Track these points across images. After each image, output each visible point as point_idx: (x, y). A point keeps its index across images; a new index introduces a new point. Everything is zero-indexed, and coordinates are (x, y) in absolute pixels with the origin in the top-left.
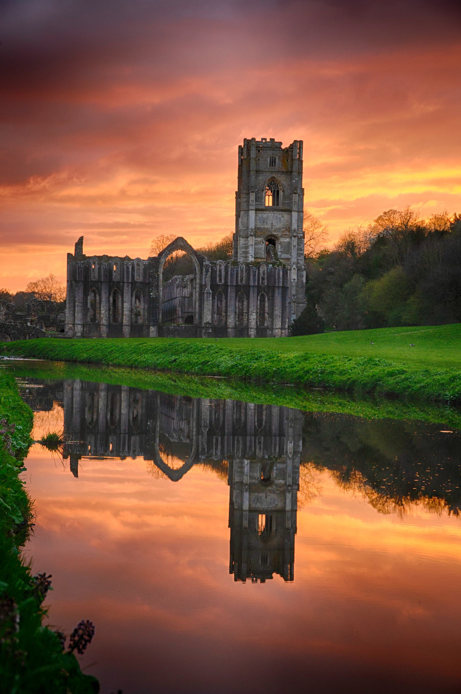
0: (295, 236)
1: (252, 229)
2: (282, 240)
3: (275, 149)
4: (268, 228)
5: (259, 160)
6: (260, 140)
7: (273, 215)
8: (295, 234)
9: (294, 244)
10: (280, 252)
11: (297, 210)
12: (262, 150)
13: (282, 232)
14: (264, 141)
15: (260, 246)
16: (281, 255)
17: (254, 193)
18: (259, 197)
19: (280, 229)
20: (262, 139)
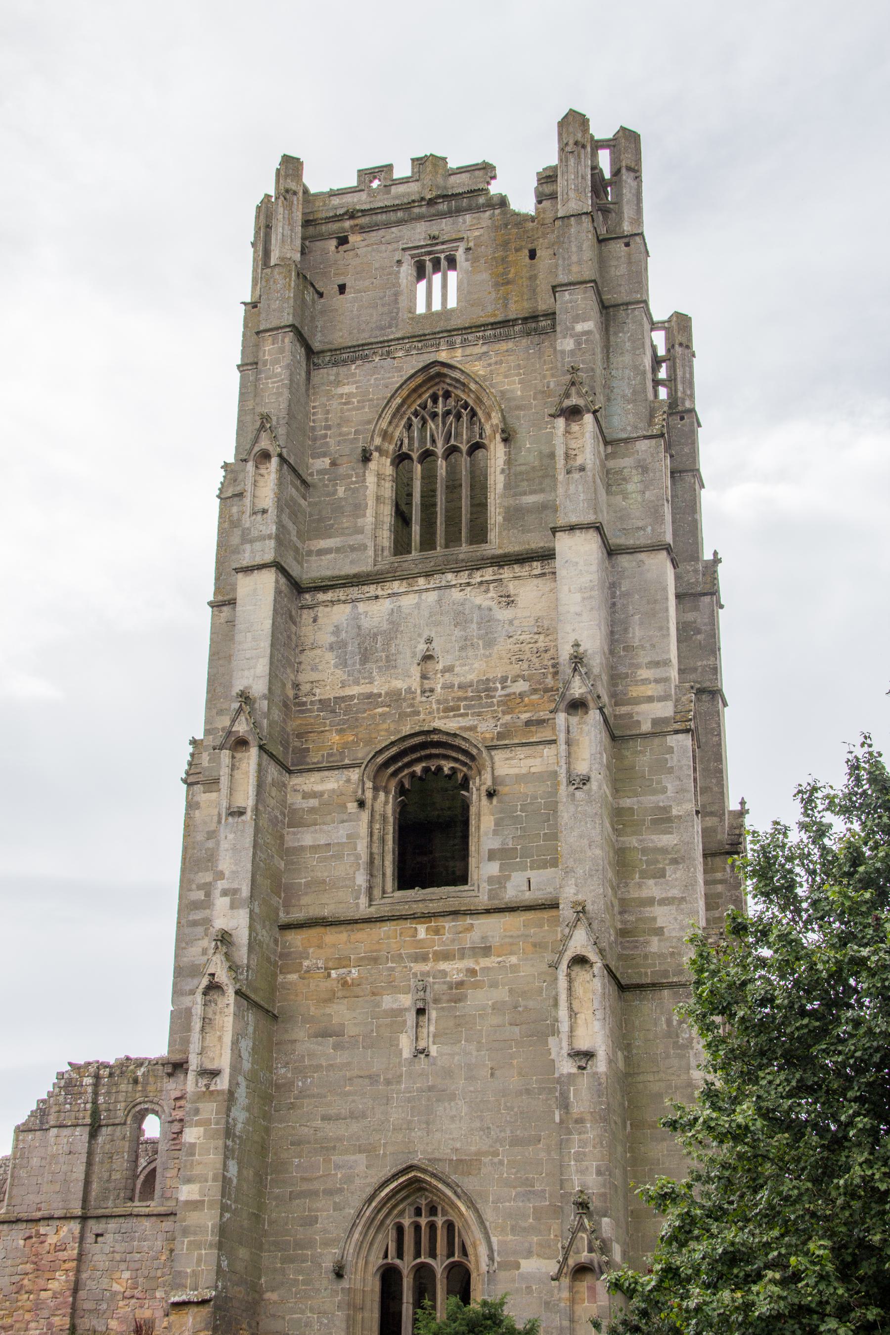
0: (577, 706)
1: (245, 698)
2: (507, 765)
3: (443, 207)
4: (395, 697)
5: (342, 289)
6: (354, 183)
7: (432, 597)
8: (577, 689)
9: (582, 767)
10: (492, 855)
11: (590, 518)
12: (363, 230)
13: (510, 703)
14: (375, 184)
15: (338, 833)
16: (499, 882)
17: (275, 461)
18: (338, 509)
19: (486, 688)
20: (368, 175)
